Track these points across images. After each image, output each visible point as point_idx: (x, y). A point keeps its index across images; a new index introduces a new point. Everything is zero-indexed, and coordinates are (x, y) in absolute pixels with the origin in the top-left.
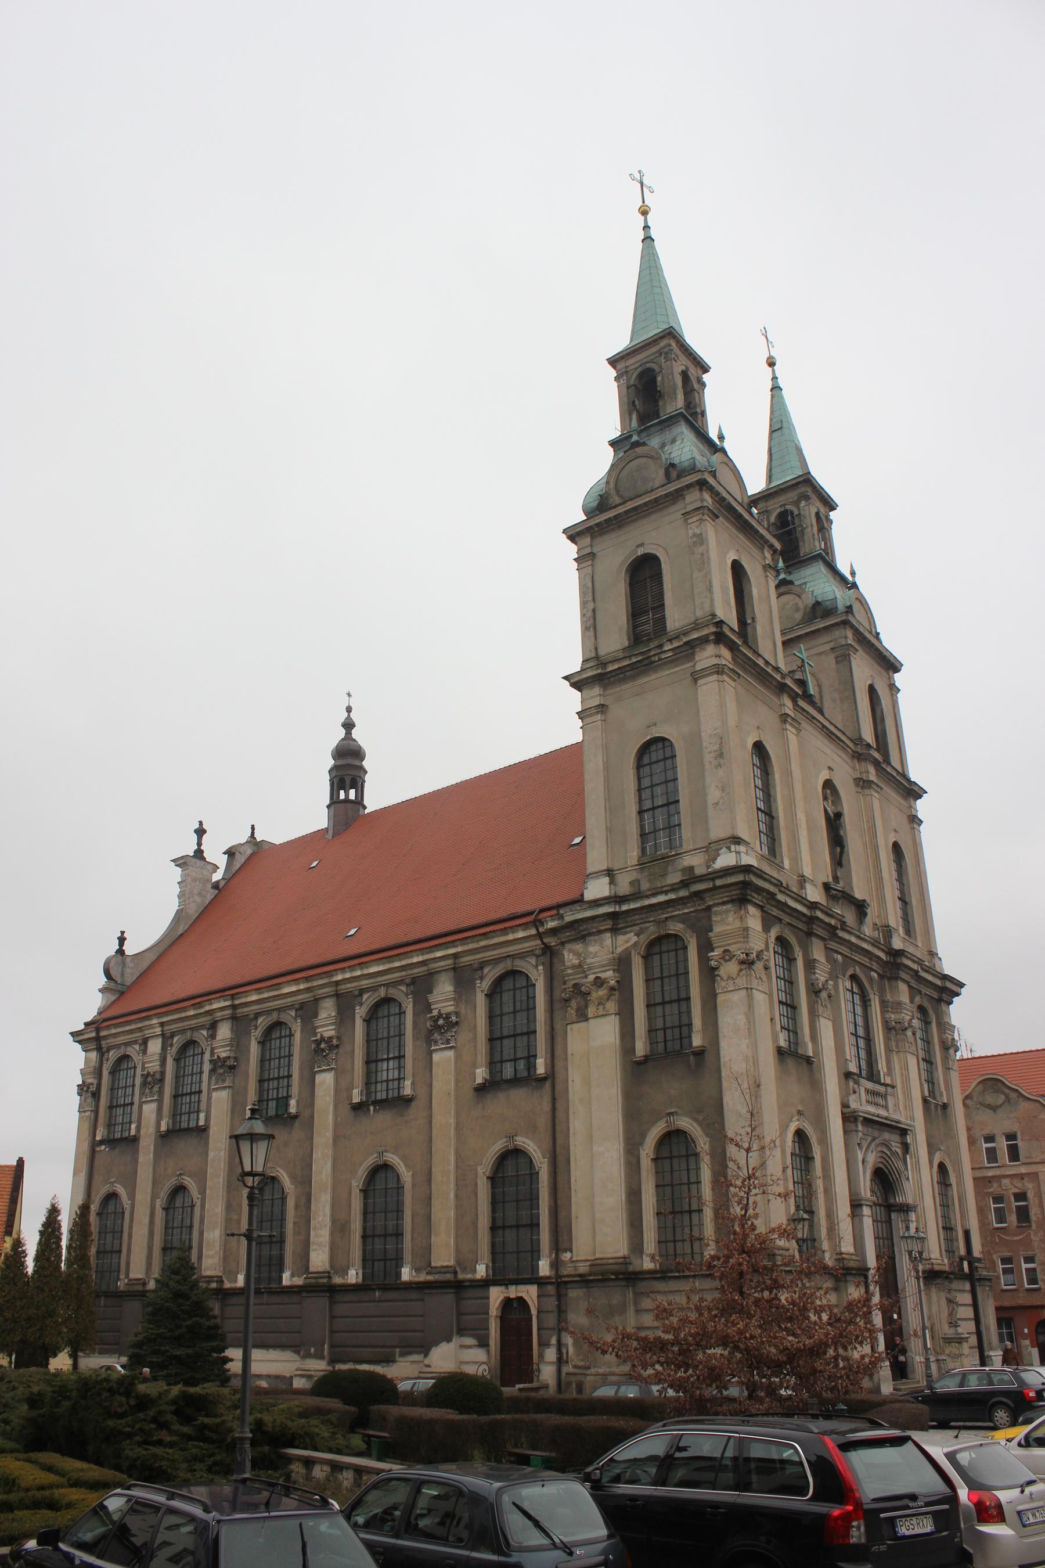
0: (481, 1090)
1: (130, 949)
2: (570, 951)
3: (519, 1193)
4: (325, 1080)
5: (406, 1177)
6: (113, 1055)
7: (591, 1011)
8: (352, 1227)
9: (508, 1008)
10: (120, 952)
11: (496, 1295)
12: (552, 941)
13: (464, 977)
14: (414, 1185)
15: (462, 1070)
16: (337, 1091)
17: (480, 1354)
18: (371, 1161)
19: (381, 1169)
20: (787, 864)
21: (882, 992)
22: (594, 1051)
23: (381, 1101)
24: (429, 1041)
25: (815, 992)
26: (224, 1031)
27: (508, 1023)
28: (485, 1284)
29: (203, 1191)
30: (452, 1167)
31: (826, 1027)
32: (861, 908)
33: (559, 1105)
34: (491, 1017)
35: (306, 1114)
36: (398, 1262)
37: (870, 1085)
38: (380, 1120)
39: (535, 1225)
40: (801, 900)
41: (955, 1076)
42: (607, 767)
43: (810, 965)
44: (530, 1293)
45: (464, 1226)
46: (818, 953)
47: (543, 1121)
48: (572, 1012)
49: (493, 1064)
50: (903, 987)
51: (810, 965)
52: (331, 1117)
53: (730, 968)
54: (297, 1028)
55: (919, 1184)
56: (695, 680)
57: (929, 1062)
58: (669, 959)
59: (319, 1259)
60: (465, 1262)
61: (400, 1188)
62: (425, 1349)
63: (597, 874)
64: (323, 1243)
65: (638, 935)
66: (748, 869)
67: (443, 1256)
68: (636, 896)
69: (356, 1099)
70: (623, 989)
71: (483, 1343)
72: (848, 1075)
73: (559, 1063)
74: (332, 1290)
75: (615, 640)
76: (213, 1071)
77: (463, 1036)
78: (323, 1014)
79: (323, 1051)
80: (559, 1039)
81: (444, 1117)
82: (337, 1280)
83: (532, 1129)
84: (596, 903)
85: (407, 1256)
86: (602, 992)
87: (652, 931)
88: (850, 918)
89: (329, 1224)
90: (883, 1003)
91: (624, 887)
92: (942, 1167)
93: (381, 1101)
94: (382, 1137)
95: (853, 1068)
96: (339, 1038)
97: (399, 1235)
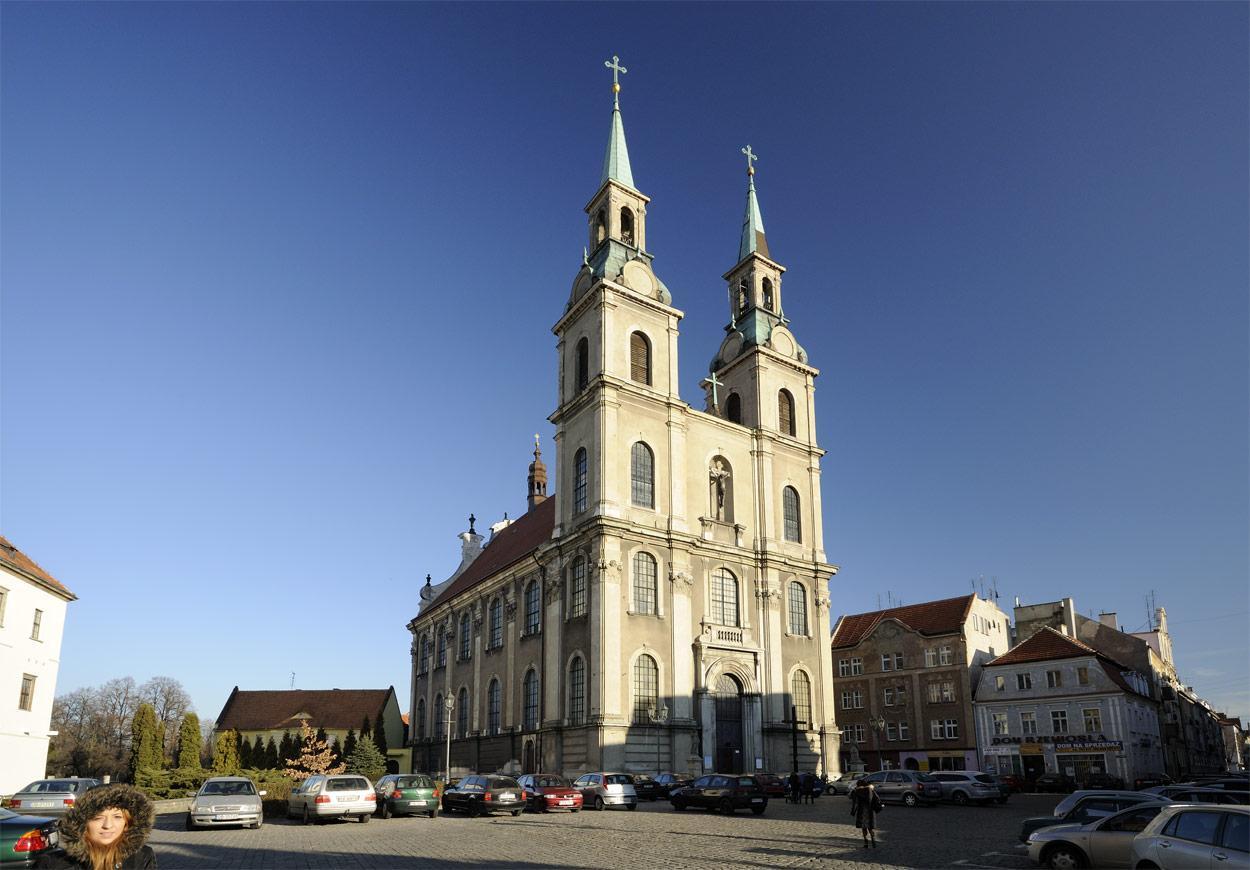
1: (432, 583)
6: (421, 635)
10: (428, 585)
62: (502, 765)
67: (509, 724)
71: (520, 763)
75: (569, 394)
93: (494, 650)
96: (482, 619)
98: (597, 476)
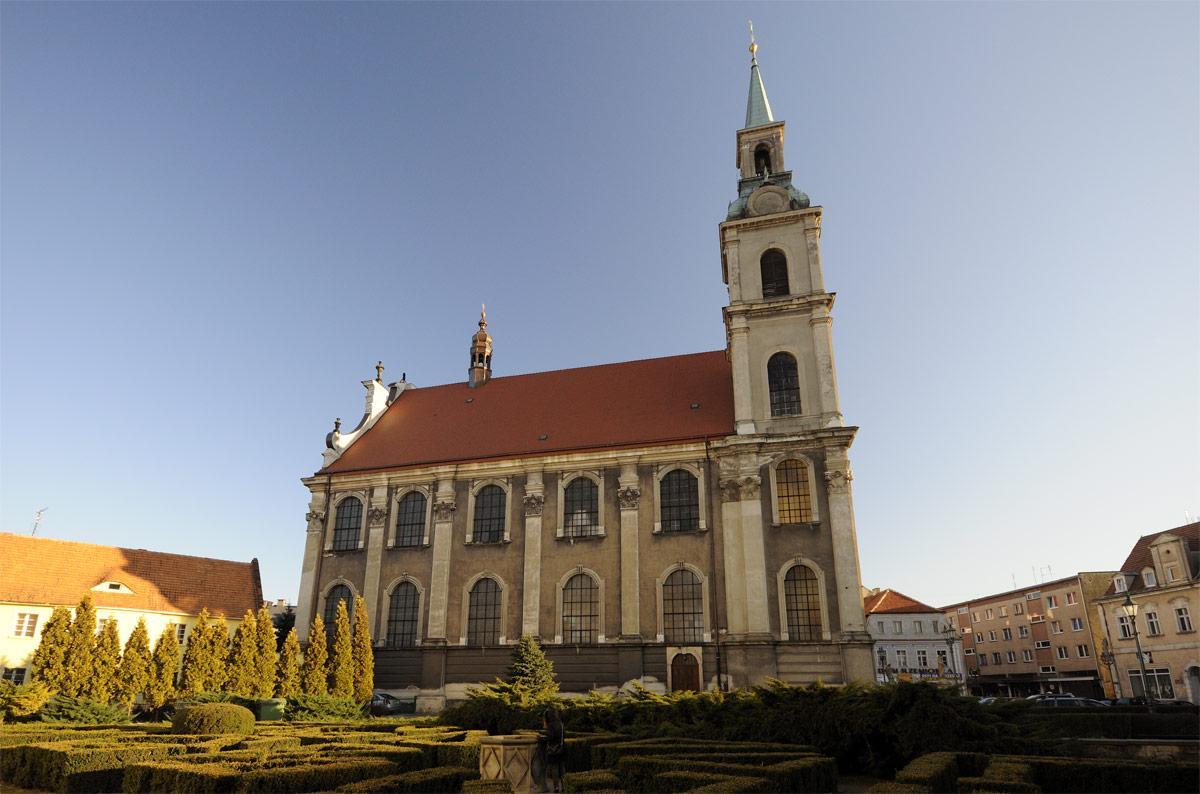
2: (725, 462)
4: (534, 523)
5: (600, 582)
7: (742, 496)
8: (557, 610)
14: (606, 588)
30: (638, 578)
33: (717, 548)
47: (704, 555)
52: (539, 545)
54: (509, 491)
56: (813, 324)
65: (773, 457)
70: (764, 486)
79: (529, 506)
80: (715, 510)
83: (697, 559)
86: (751, 486)
89: (538, 609)
91: (763, 430)
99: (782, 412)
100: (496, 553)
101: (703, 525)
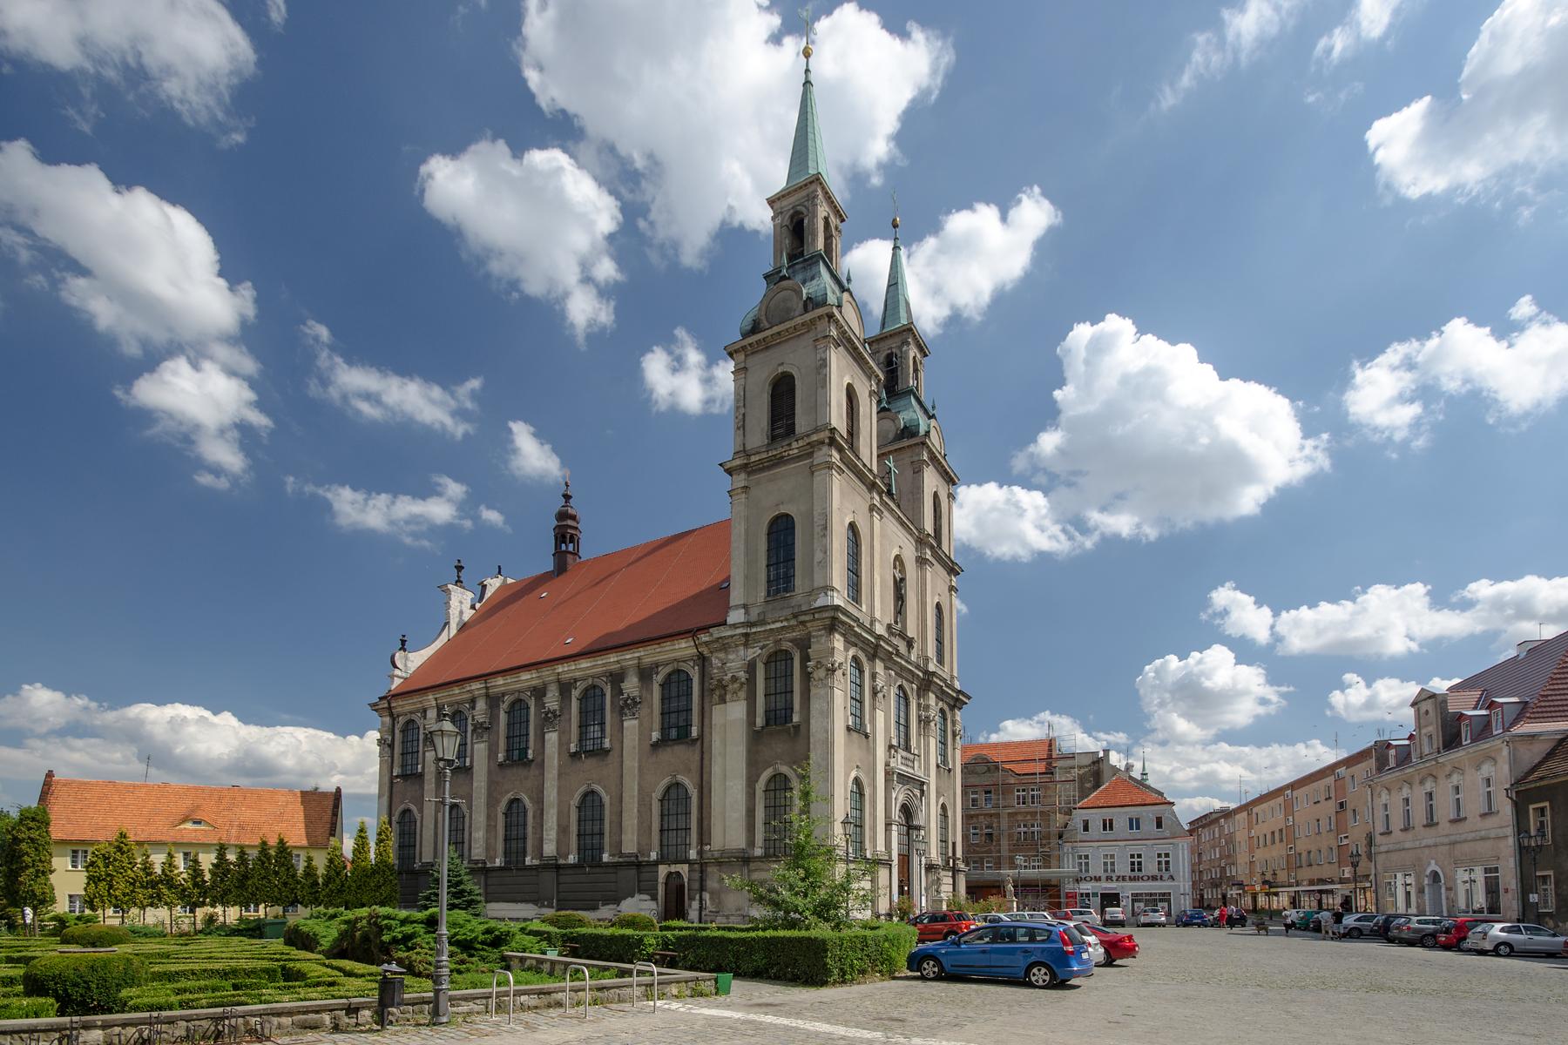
0: (655, 746)
3: (680, 808)
4: (552, 737)
5: (606, 799)
9: (674, 694)
11: (663, 870)
12: (705, 651)
13: (645, 674)
15: (644, 733)
16: (560, 744)
17: (653, 905)
18: (582, 789)
19: (590, 795)
20: (864, 608)
21: (919, 697)
22: (730, 721)
23: (590, 751)
24: (622, 713)
25: (875, 693)
26: (481, 705)
27: (674, 705)
28: (656, 863)
29: (470, 807)
31: (880, 715)
32: (910, 643)
34: (664, 699)
35: (539, 759)
36: (601, 850)
37: (905, 754)
38: (589, 764)
39: (688, 829)
40: (871, 632)
41: (958, 752)
42: (747, 531)
43: (874, 676)
44: (683, 869)
45: (643, 828)
46: (879, 667)
47: (695, 766)
48: (716, 697)
49: (664, 730)
50: (932, 696)
51: (874, 676)
53: (821, 673)
54: (532, 704)
55: (929, 815)
57: (944, 743)
58: (781, 666)
59: (550, 849)
60: (644, 850)
61: (602, 806)
62: (617, 901)
63: (737, 607)
64: (552, 838)
66: (837, 608)
68: (762, 622)
69: (573, 750)
70: (751, 681)
71: (654, 898)
72: (891, 747)
73: (706, 729)
74: (558, 867)
76: (474, 731)
77: (644, 711)
78: (549, 695)
79: (549, 719)
81: (631, 763)
82: (561, 861)
84: (734, 626)
85: (607, 847)
86: (736, 685)
87: (771, 648)
88: (903, 648)
90: (919, 705)
91: (754, 617)
92: (944, 807)
93: (590, 751)
94: (590, 774)
95: (894, 742)
97: (601, 834)
98: (818, 556)
99: (778, 591)
100: (522, 772)
101: (695, 732)
